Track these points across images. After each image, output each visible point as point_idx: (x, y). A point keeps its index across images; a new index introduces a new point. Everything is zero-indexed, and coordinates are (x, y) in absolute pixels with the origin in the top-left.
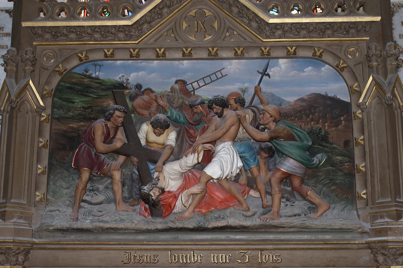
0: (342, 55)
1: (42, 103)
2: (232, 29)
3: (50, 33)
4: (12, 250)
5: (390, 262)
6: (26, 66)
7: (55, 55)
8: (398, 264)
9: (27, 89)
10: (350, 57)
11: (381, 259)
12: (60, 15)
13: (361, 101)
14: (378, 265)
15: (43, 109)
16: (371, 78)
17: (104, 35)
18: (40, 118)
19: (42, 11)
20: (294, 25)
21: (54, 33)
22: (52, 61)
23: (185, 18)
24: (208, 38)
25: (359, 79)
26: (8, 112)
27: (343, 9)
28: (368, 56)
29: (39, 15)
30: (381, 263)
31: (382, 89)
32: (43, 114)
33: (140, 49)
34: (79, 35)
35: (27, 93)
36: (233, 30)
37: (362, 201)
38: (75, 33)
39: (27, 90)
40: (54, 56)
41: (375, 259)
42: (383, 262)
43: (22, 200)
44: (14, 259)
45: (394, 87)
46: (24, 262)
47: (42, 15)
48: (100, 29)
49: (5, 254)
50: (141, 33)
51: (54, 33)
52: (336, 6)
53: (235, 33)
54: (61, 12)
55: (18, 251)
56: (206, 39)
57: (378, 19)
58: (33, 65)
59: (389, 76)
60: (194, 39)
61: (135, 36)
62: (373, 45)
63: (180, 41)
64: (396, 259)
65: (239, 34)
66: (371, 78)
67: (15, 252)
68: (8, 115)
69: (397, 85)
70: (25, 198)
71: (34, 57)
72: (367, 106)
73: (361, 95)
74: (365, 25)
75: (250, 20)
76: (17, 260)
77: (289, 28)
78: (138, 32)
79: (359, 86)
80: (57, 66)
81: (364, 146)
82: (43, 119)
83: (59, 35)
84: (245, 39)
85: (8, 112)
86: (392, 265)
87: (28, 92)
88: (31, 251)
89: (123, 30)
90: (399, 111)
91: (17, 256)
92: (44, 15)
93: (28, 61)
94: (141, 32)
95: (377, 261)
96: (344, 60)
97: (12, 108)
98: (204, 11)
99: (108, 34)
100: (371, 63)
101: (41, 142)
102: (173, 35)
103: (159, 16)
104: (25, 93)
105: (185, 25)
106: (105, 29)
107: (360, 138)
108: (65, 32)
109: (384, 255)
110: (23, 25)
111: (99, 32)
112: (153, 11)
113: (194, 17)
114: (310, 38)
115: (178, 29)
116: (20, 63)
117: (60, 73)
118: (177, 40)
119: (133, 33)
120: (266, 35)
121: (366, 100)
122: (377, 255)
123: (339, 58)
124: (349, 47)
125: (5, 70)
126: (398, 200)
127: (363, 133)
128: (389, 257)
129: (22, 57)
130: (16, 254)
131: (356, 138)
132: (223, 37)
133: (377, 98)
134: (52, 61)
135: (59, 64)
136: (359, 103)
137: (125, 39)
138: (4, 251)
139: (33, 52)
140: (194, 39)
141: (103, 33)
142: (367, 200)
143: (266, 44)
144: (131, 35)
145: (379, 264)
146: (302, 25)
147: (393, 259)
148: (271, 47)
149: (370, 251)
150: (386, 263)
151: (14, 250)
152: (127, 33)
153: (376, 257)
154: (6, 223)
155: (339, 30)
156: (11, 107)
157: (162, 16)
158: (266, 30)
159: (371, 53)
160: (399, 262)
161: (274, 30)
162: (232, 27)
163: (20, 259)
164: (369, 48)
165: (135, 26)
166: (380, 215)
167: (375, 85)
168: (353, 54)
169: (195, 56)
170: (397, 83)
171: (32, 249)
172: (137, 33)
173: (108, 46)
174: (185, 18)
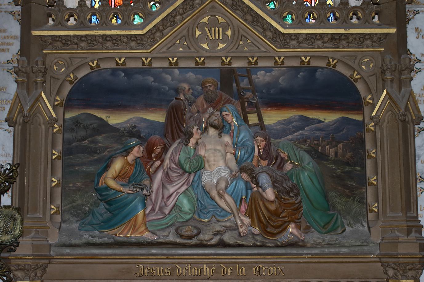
0: (355, 66)
1: (54, 116)
2: (245, 37)
3: (60, 41)
4: (31, 266)
5: (400, 276)
6: (37, 77)
7: (67, 66)
8: (407, 278)
9: (39, 101)
10: (364, 67)
11: (391, 272)
12: (69, 20)
13: (374, 114)
14: (388, 278)
15: (56, 121)
16: (385, 92)
17: (115, 43)
18: (53, 130)
19: (51, 16)
20: (309, 36)
21: (64, 41)
22: (63, 70)
23: (198, 26)
24: (221, 46)
25: (373, 92)
26: (20, 125)
27: (358, 17)
28: (382, 67)
29: (48, 22)
30: (391, 277)
31: (395, 104)
32: (56, 125)
33: (152, 58)
34: (90, 43)
35: (39, 105)
36: (247, 38)
37: (373, 213)
38: (86, 41)
39: (39, 102)
40: (65, 65)
41: (385, 271)
42: (393, 276)
43: (38, 214)
44: (33, 274)
45: (408, 100)
46: (42, 277)
47: (51, 22)
48: (112, 38)
49: (24, 270)
50: (154, 41)
51: (64, 41)
52: (351, 14)
53: (249, 41)
54: (70, 17)
55: (37, 267)
56: (219, 48)
57: (393, 30)
58: (44, 75)
59: (403, 90)
60: (207, 48)
61: (147, 45)
62: (388, 57)
63: (193, 50)
64: (406, 273)
65: (252, 43)
66: (385, 92)
67: (34, 268)
68: (20, 128)
69: (411, 98)
70: (41, 212)
71: (45, 68)
72: (380, 120)
73: (374, 108)
74: (380, 37)
75: (264, 30)
76: (36, 275)
77: (304, 38)
78: (150, 41)
79: (372, 99)
80: (68, 76)
81: (376, 159)
82: (55, 130)
83: (69, 44)
84: (259, 48)
85: (20, 125)
86: (402, 279)
87: (40, 104)
88: (49, 265)
89: (136, 39)
90: (411, 124)
91: (34, 271)
92: (53, 20)
93: (39, 71)
94: (153, 41)
95: (387, 274)
96: (357, 71)
97: (25, 123)
98: (217, 18)
99: (120, 43)
100: (385, 77)
101: (55, 154)
102: (185, 43)
103: (171, 23)
104: (38, 104)
105: (198, 33)
106: (117, 38)
107: (373, 152)
108: (75, 40)
109: (394, 269)
110: (33, 34)
111: (111, 41)
112: (165, 19)
113: (207, 24)
114: (325, 48)
115: (191, 37)
116: (31, 74)
117: (71, 82)
118: (190, 49)
119: (145, 42)
120: (280, 45)
121: (379, 114)
122: (387, 269)
123: (354, 70)
124: (364, 57)
125: (16, 81)
126: (408, 215)
127: (376, 146)
128: (399, 271)
129: (34, 68)
130: (35, 270)
131: (369, 150)
132: (236, 47)
133: (390, 112)
134: (63, 70)
135: (70, 73)
136: (373, 116)
137: (137, 47)
138: (23, 267)
139: (44, 62)
140: (207, 48)
141: (114, 42)
142: (378, 214)
143: (280, 54)
144: (142, 44)
145: (389, 277)
146: (317, 35)
147: (402, 273)
148: (285, 57)
149: (380, 264)
150: (396, 277)
151: (33, 267)
152: (139, 42)
153: (386, 270)
154: (24, 239)
155: (354, 41)
156: (24, 121)
157: (174, 24)
158: (280, 40)
159: (385, 68)
160: (408, 276)
161: (288, 40)
162: (245, 34)
163: (39, 275)
164: (383, 60)
165: (147, 36)
166: (391, 230)
167: (389, 98)
168: (367, 65)
169: (207, 65)
170: (411, 96)
171: (49, 263)
172: (149, 41)
173: (119, 55)
174: (199, 24)
